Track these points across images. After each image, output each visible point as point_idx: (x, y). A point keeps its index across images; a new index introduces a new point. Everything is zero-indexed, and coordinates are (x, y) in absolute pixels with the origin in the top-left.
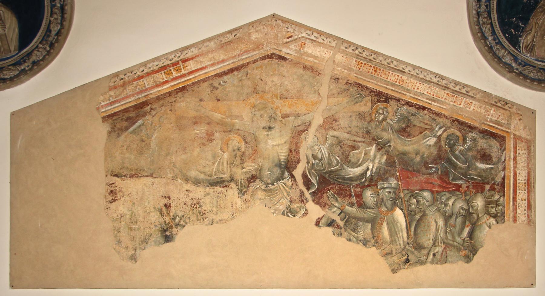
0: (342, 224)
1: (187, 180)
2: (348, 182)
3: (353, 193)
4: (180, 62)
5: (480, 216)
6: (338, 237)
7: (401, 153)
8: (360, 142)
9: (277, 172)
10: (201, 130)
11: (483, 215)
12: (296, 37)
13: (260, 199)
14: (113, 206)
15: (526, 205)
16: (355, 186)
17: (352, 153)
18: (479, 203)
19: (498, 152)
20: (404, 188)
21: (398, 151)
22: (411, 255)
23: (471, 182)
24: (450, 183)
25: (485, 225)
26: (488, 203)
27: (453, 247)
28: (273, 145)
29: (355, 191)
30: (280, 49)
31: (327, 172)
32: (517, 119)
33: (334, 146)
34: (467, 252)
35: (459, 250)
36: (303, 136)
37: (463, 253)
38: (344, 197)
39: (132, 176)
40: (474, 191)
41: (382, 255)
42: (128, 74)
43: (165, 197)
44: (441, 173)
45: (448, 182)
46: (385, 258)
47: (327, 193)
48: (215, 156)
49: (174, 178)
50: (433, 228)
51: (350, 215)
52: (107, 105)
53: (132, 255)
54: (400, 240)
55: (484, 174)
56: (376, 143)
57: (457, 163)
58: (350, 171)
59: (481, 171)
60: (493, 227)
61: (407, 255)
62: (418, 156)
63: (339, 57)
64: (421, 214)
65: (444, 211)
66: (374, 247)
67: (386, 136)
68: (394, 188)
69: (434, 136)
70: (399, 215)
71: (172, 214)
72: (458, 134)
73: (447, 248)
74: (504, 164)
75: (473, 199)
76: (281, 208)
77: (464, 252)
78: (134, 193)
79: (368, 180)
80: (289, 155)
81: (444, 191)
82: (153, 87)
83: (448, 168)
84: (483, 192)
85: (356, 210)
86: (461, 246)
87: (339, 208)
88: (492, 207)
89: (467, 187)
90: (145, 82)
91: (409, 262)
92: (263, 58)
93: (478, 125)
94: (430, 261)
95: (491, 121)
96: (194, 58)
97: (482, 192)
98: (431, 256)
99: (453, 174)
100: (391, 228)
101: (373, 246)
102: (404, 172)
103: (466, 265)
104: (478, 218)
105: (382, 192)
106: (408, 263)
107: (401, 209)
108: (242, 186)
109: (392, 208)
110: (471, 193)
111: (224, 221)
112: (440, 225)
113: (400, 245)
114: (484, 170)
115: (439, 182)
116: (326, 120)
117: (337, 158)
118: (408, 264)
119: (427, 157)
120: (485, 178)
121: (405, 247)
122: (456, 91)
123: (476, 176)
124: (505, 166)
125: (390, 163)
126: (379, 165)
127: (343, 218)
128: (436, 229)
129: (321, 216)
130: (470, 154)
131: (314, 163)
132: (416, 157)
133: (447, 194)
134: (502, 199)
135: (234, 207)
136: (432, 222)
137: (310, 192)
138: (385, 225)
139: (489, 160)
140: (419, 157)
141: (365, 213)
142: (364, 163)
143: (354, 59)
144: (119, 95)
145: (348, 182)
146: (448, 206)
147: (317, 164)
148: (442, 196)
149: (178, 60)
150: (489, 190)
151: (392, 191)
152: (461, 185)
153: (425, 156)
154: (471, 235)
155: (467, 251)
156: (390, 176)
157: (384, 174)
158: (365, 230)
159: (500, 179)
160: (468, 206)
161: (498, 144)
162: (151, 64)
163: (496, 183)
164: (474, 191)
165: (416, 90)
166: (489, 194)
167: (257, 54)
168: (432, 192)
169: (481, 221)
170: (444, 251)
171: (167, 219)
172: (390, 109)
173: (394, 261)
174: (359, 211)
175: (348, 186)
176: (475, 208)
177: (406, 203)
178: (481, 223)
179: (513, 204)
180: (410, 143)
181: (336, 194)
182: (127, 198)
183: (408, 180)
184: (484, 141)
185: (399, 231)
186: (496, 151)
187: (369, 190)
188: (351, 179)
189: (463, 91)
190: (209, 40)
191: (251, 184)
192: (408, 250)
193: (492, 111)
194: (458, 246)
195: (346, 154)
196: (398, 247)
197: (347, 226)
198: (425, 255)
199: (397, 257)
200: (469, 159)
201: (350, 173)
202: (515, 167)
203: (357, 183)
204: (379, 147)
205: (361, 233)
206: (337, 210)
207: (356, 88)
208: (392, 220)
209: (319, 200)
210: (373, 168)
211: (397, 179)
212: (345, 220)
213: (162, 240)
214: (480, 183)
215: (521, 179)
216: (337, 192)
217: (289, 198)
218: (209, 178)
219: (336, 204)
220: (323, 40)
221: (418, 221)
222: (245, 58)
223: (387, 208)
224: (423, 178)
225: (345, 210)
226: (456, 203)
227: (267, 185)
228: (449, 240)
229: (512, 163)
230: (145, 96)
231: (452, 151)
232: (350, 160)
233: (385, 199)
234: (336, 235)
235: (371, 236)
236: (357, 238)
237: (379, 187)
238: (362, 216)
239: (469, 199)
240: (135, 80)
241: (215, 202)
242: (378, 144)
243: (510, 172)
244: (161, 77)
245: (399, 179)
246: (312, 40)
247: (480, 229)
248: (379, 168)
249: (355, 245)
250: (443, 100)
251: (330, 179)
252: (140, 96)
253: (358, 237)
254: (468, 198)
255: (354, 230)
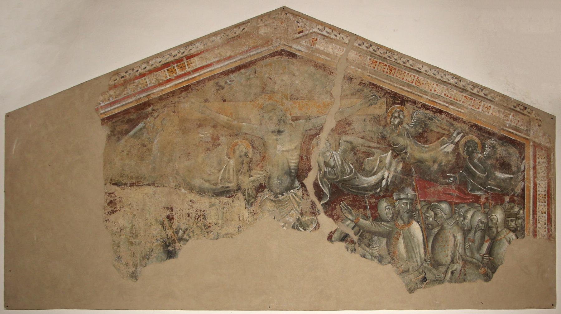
0: (355, 238)
1: (191, 189)
2: (362, 192)
3: (368, 205)
4: (185, 59)
5: (500, 230)
6: (352, 253)
7: (418, 161)
8: (374, 148)
9: (287, 181)
10: (206, 134)
11: (502, 230)
12: (307, 32)
13: (269, 211)
14: (113, 217)
15: (546, 218)
16: (370, 197)
17: (366, 160)
18: (498, 217)
19: (518, 160)
20: (421, 199)
21: (415, 158)
22: (429, 273)
23: (490, 193)
24: (469, 194)
25: (504, 240)
26: (508, 216)
27: (472, 265)
28: (283, 151)
29: (369, 202)
30: (290, 45)
31: (340, 181)
32: (537, 125)
33: (347, 153)
34: (486, 270)
35: (478, 267)
36: (314, 141)
37: (482, 271)
38: (358, 209)
39: (132, 185)
40: (494, 203)
41: (398, 273)
42: (129, 72)
43: (168, 208)
44: (460, 183)
45: (466, 192)
46: (401, 276)
47: (341, 204)
48: (220, 163)
49: (177, 187)
50: (451, 243)
51: (365, 229)
52: (107, 106)
53: (133, 273)
54: (417, 257)
55: (503, 185)
56: (391, 150)
57: (476, 172)
58: (364, 180)
59: (500, 181)
60: (512, 242)
61: (425, 273)
62: (436, 163)
63: (352, 55)
64: (439, 228)
65: (463, 224)
66: (390, 265)
67: (402, 141)
68: (411, 199)
69: (452, 143)
70: (416, 228)
71: (174, 228)
72: (477, 140)
73: (466, 266)
74: (523, 174)
75: (492, 212)
76: (291, 220)
77: (483, 270)
78: (135, 204)
79: (383, 190)
80: (299, 162)
81: (462, 203)
82: (155, 87)
83: (467, 178)
84: (503, 204)
85: (371, 223)
86: (480, 263)
87: (352, 221)
88: (512, 221)
89: (485, 198)
90: (147, 80)
91: (426, 280)
92: (273, 55)
93: (497, 131)
94: (448, 279)
95: (510, 127)
96: (199, 54)
97: (501, 204)
98: (449, 275)
99: (472, 184)
100: (408, 243)
101: (389, 263)
102: (421, 181)
103: (486, 284)
104: (498, 233)
105: (399, 203)
106: (425, 282)
107: (418, 222)
108: (249, 196)
109: (408, 221)
110: (490, 204)
111: (230, 235)
112: (458, 240)
113: (417, 262)
114: (504, 180)
115: (457, 193)
116: (339, 124)
117: (351, 165)
118: (425, 283)
119: (445, 165)
120: (505, 188)
121: (422, 264)
122: (474, 94)
123: (495, 187)
124: (524, 175)
125: (406, 171)
126: (395, 174)
127: (357, 232)
128: (454, 244)
129: (333, 230)
130: (489, 162)
131: (327, 171)
132: (433, 165)
133: (466, 205)
134: (521, 212)
135: (241, 219)
136: (450, 237)
137: (322, 203)
138: (401, 240)
139: (509, 169)
140: (437, 165)
141: (380, 227)
142: (379, 171)
143: (369, 57)
144: (120, 95)
145: (362, 192)
146: (466, 219)
147: (329, 172)
148: (461, 208)
149: (182, 56)
150: (509, 202)
151: (408, 203)
152: (480, 196)
153: (443, 164)
154: (490, 251)
155: (486, 268)
156: (406, 186)
157: (400, 183)
158: (380, 245)
159: (520, 190)
160: (487, 219)
161: (518, 152)
162: (154, 61)
163: (516, 195)
164: (494, 203)
165: (433, 91)
166: (509, 207)
167: (265, 50)
168: (450, 204)
169: (500, 236)
170: (463, 269)
171: (170, 233)
172: (406, 112)
173: (411, 280)
174: (374, 225)
175: (362, 197)
176: (494, 221)
177: (423, 215)
178: (501, 237)
179: (534, 217)
180: (427, 150)
181: (349, 205)
182: (127, 209)
183: (425, 190)
184: (503, 148)
185: (416, 247)
186: (515, 160)
187: (384, 201)
188: (365, 189)
189: (481, 94)
190: (215, 34)
191: (259, 194)
192: (425, 267)
193: (511, 116)
194: (477, 263)
195: (360, 161)
196: (415, 264)
197: (361, 241)
198: (443, 273)
199: (414, 275)
200: (488, 168)
201: (365, 182)
202: (535, 177)
203: (372, 193)
204: (395, 154)
205: (376, 248)
206: (350, 223)
207: (370, 89)
208: (409, 234)
209: (332, 212)
210: (388, 177)
211: (414, 190)
212: (359, 234)
213: (164, 257)
214: (499, 195)
215: (541, 190)
216: (350, 203)
217: (299, 209)
218: (214, 187)
219: (350, 217)
220: (336, 36)
221: (436, 235)
222: (253, 54)
223: (403, 221)
224: (440, 188)
225: (359, 223)
226: (475, 216)
227: (276, 195)
228: (468, 256)
229: (531, 173)
230: (147, 96)
231: (471, 159)
232: (364, 168)
233: (401, 211)
234: (349, 250)
235: (387, 252)
236: (372, 254)
237: (395, 198)
238: (377, 230)
239: (488, 212)
240: (136, 78)
241: (220, 214)
242: (394, 151)
243: (530, 182)
244: (164, 75)
245: (416, 189)
246: (324, 35)
247: (499, 244)
248: (395, 177)
249: (370, 262)
250: (461, 103)
251: (343, 189)
252: (141, 96)
253: (372, 253)
254: (487, 210)
255: (369, 246)
